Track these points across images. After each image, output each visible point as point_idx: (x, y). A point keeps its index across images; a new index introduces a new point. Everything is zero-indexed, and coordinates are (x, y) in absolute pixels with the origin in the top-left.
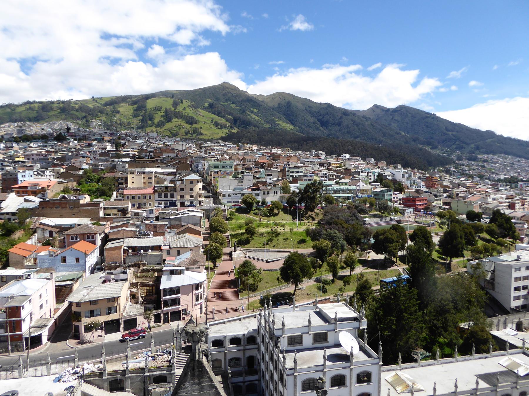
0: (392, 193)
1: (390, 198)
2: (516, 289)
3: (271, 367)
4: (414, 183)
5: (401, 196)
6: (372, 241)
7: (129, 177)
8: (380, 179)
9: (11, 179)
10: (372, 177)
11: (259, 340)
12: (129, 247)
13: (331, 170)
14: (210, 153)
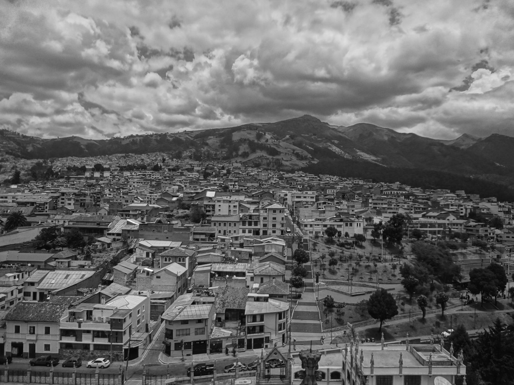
1: (486, 233)
7: (217, 204)
9: (116, 203)
10: (464, 211)
11: (344, 376)
13: (418, 202)
14: (291, 183)
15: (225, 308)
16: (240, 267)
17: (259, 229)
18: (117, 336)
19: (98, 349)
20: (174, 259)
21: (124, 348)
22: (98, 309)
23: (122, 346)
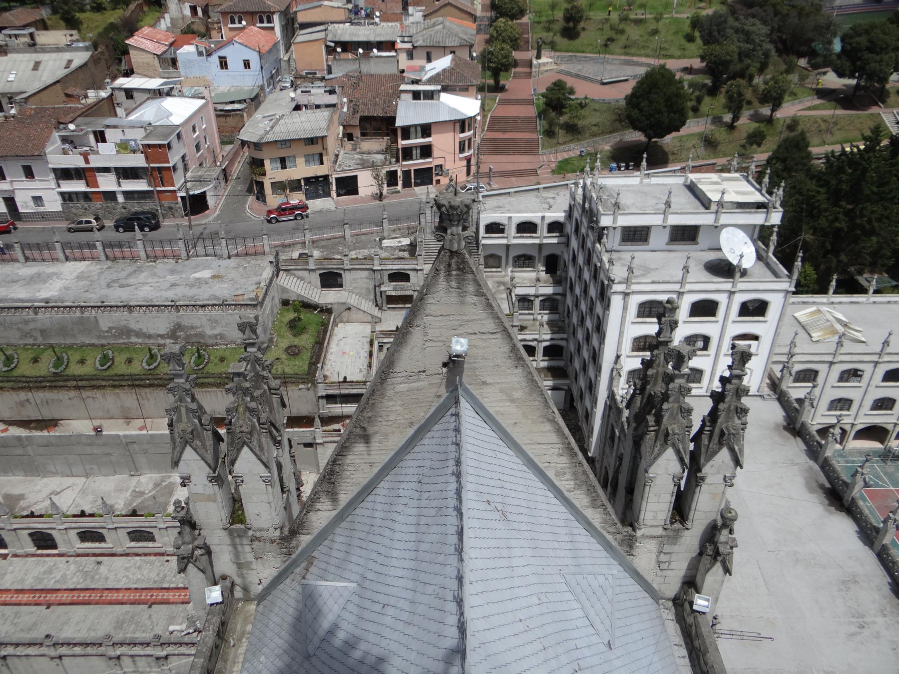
3: (586, 275)
6: (837, 46)
11: (569, 229)
12: (337, 43)
15: (358, 116)
16: (382, 31)
18: (161, 175)
19: (134, 199)
20: (249, 17)
21: (179, 194)
22: (115, 127)
23: (174, 191)
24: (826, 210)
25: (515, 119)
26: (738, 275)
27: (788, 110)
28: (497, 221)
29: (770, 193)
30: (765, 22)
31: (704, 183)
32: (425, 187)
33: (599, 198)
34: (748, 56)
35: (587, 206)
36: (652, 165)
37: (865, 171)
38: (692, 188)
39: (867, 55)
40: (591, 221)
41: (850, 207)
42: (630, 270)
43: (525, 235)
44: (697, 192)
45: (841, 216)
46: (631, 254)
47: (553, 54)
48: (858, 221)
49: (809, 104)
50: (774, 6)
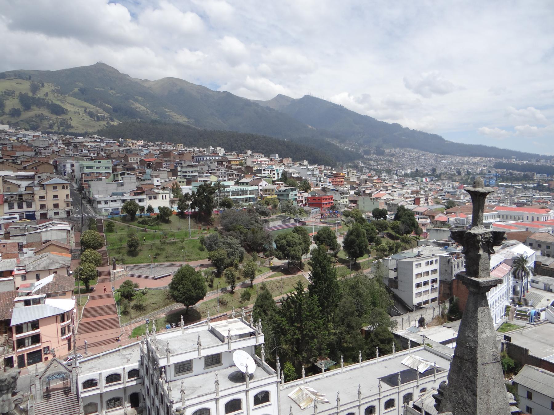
0: (296, 192)
1: (295, 197)
2: (418, 285)
3: (157, 403)
4: (320, 181)
5: (306, 195)
6: (274, 246)
8: (285, 177)
10: (276, 175)
11: (143, 373)
14: (82, 151)
17: (34, 211)
24: (289, 329)
25: (102, 308)
26: (247, 379)
27: (259, 280)
28: (91, 378)
29: (255, 326)
30: (237, 238)
31: (218, 327)
32: (34, 365)
33: (157, 348)
34: (232, 255)
35: (150, 355)
36: (187, 322)
37: (300, 305)
38: (213, 331)
39: (288, 248)
40: (154, 364)
41: (299, 325)
42: (182, 392)
43: (112, 384)
44: (216, 333)
45: (297, 331)
46: (181, 381)
47: (123, 266)
48: (305, 332)
49: (269, 275)
50: (239, 229)
